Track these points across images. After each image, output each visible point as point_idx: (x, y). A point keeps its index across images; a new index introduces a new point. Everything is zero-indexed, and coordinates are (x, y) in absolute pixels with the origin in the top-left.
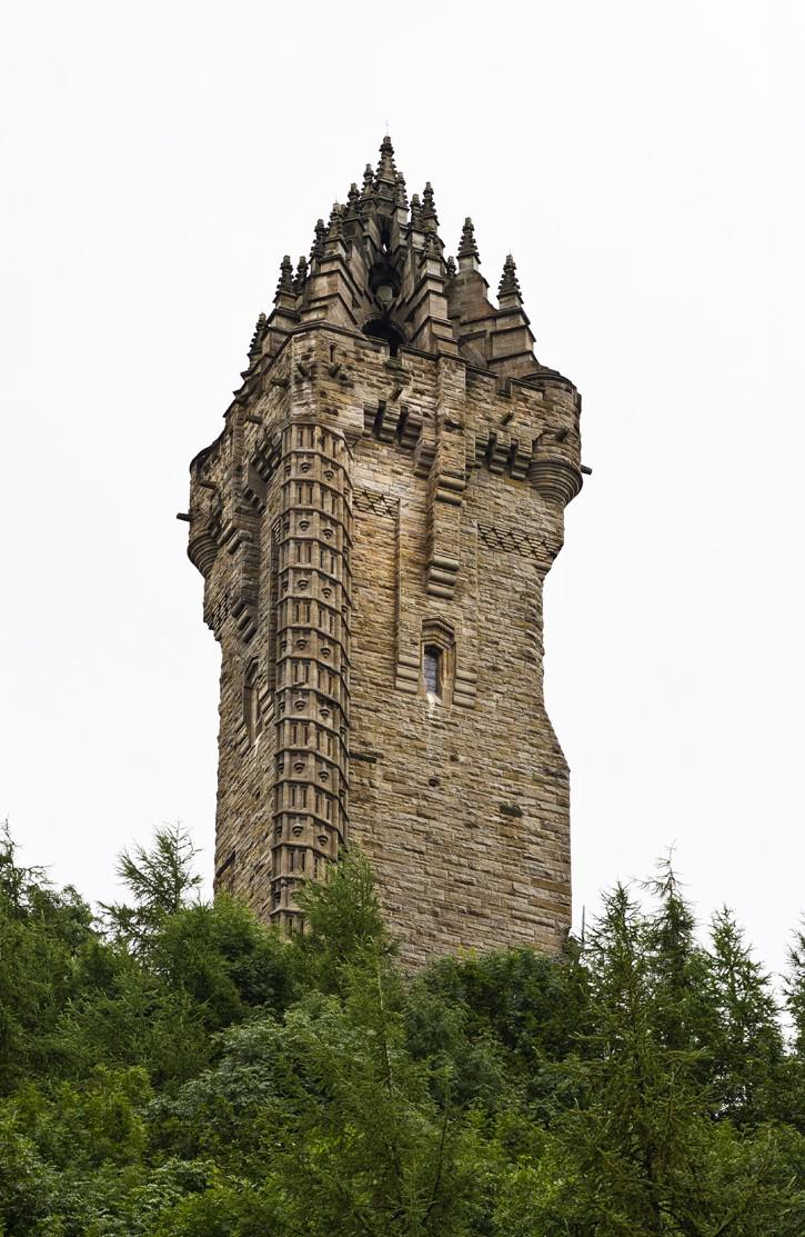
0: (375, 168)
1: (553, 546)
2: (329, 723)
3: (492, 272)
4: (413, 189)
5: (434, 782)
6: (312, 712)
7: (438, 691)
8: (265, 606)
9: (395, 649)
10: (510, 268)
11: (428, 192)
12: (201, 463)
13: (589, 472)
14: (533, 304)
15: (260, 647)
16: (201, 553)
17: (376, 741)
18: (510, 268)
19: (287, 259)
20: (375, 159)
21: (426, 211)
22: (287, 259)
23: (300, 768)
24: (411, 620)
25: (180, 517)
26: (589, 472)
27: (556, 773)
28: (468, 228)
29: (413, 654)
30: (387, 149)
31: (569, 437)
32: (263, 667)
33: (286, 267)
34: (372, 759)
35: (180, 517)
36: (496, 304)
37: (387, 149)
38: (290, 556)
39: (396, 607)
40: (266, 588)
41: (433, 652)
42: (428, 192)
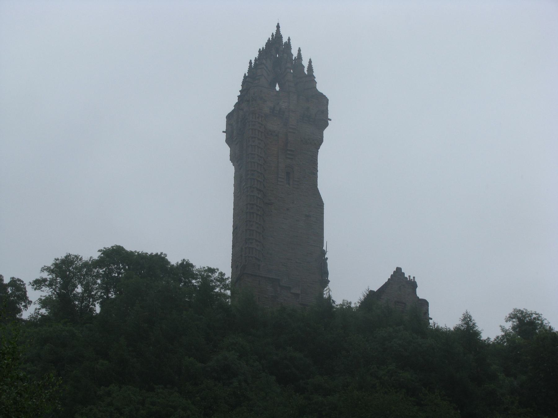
0: (274, 34)
1: (321, 141)
2: (260, 196)
3: (305, 63)
4: (285, 40)
5: (288, 210)
7: (289, 184)
10: (310, 62)
11: (289, 39)
12: (229, 117)
13: (330, 120)
14: (316, 73)
16: (229, 141)
18: (310, 62)
19: (251, 61)
20: (274, 31)
21: (288, 45)
22: (251, 61)
25: (223, 132)
26: (330, 120)
27: (320, 205)
28: (299, 50)
30: (278, 27)
31: (325, 112)
33: (250, 63)
35: (223, 132)
36: (306, 73)
37: (278, 27)
42: (289, 39)
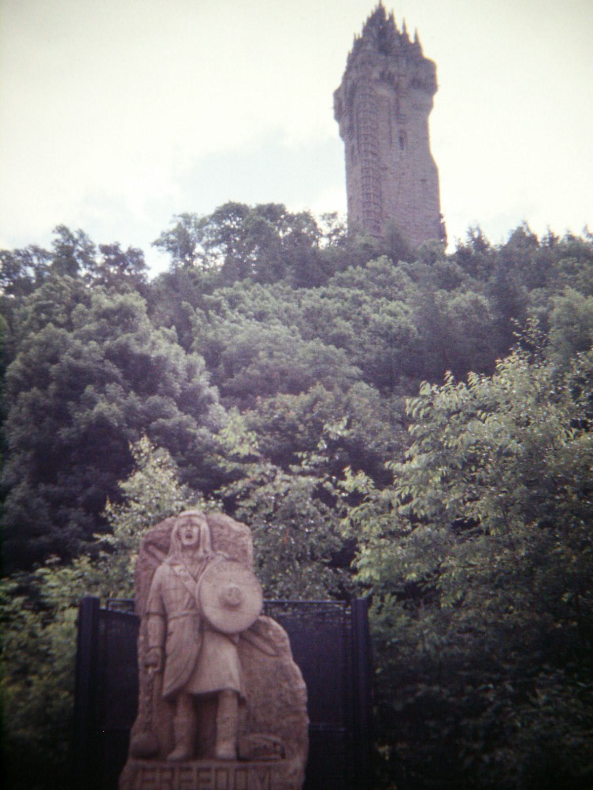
1: (429, 107)
6: (370, 157)
8: (355, 130)
9: (391, 139)
15: (355, 141)
17: (388, 165)
23: (368, 172)
24: (395, 132)
27: (434, 170)
29: (396, 140)
32: (356, 146)
34: (386, 168)
38: (361, 115)
39: (391, 128)
40: (355, 125)
41: (401, 139)
